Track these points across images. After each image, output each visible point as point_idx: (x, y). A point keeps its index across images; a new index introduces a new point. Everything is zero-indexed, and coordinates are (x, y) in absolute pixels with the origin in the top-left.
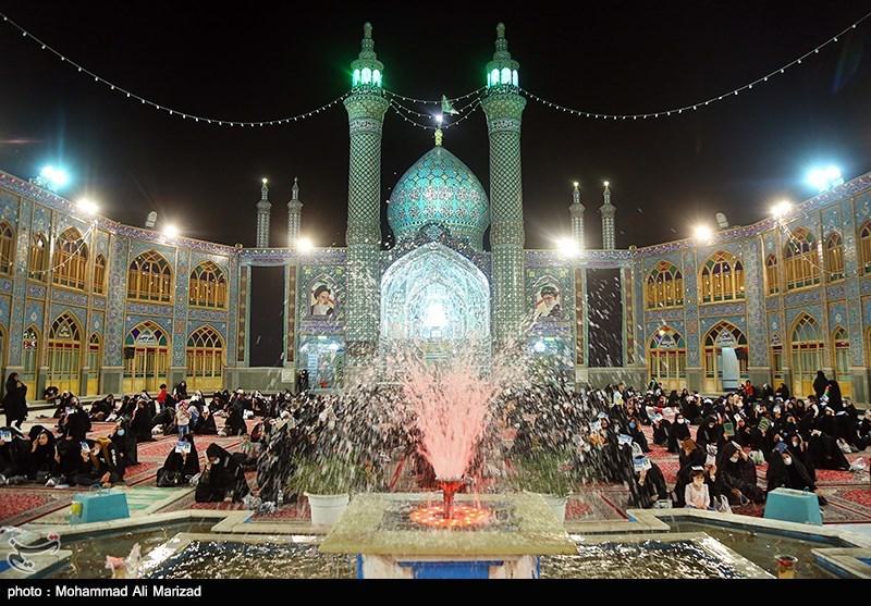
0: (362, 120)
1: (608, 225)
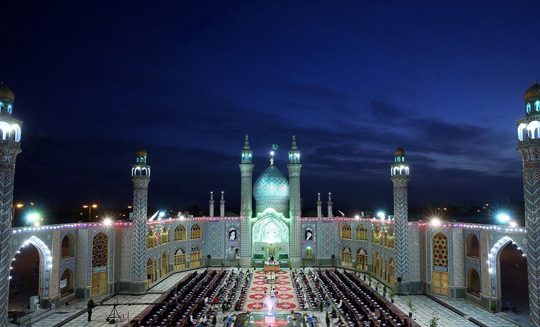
0: (245, 169)
1: (330, 208)
